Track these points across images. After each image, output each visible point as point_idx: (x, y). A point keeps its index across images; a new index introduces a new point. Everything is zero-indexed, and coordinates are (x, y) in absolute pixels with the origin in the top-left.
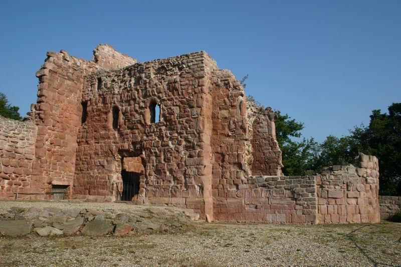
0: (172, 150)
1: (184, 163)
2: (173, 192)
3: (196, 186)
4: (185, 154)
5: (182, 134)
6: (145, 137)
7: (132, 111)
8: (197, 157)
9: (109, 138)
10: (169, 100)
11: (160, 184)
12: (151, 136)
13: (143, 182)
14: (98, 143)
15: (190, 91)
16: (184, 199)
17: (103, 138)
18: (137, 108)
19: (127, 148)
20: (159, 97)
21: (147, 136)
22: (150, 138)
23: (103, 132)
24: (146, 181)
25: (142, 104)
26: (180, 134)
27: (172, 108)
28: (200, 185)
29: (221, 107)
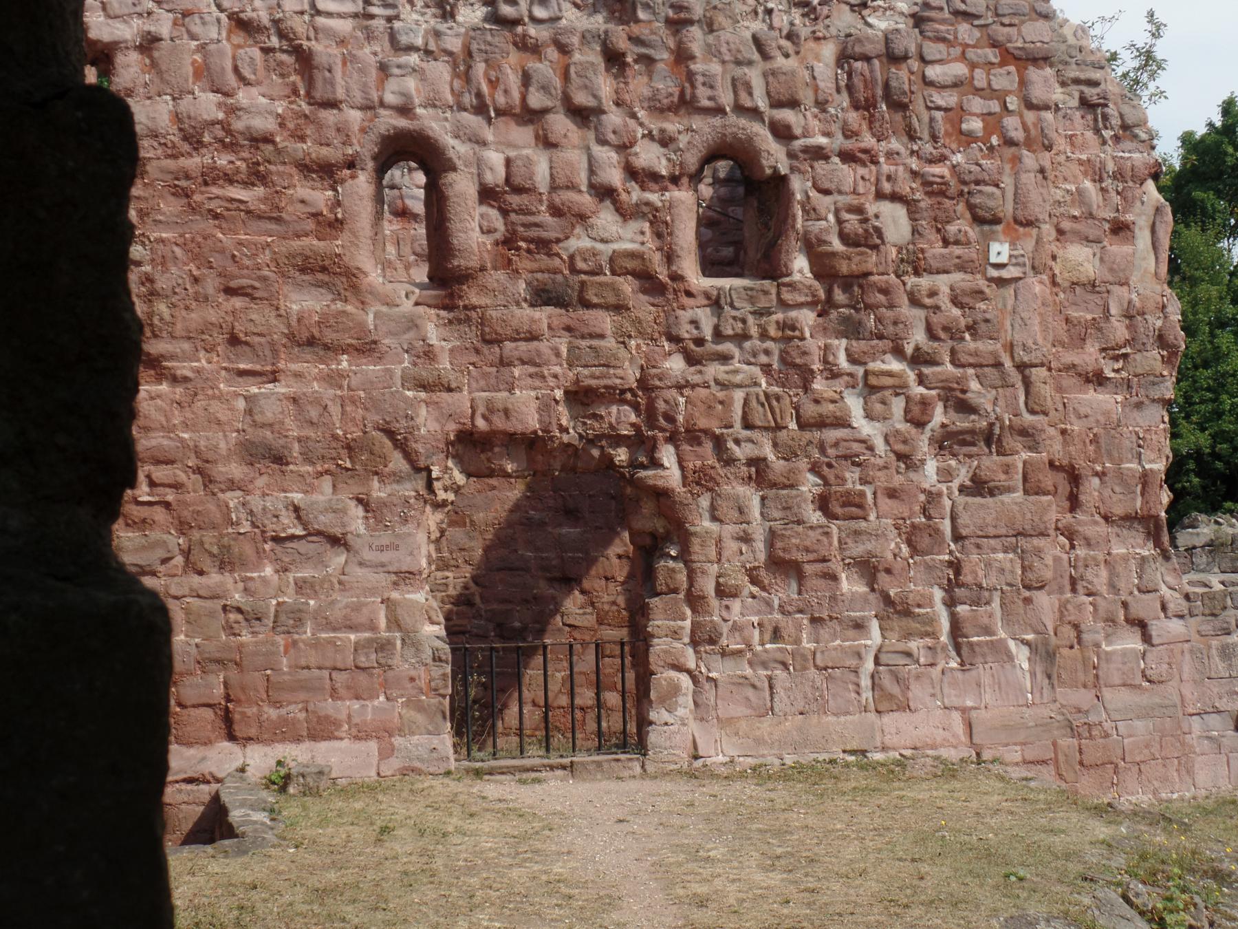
0: (871, 448)
1: (946, 526)
2: (887, 681)
3: (1012, 644)
4: (946, 475)
5: (933, 362)
6: (676, 365)
7: (572, 187)
8: (1018, 495)
9: (366, 348)
10: (847, 157)
11: (797, 641)
12: (725, 358)
13: (675, 634)
14: (274, 377)
15: (975, 125)
16: (956, 716)
17: (310, 342)
18: (614, 176)
19: (531, 421)
20: (782, 133)
21: (691, 360)
22: (714, 370)
23: (306, 302)
24: (695, 627)
25: (649, 156)
26: (919, 359)
27: (872, 208)
28: (1030, 637)
29: (1066, 225)
